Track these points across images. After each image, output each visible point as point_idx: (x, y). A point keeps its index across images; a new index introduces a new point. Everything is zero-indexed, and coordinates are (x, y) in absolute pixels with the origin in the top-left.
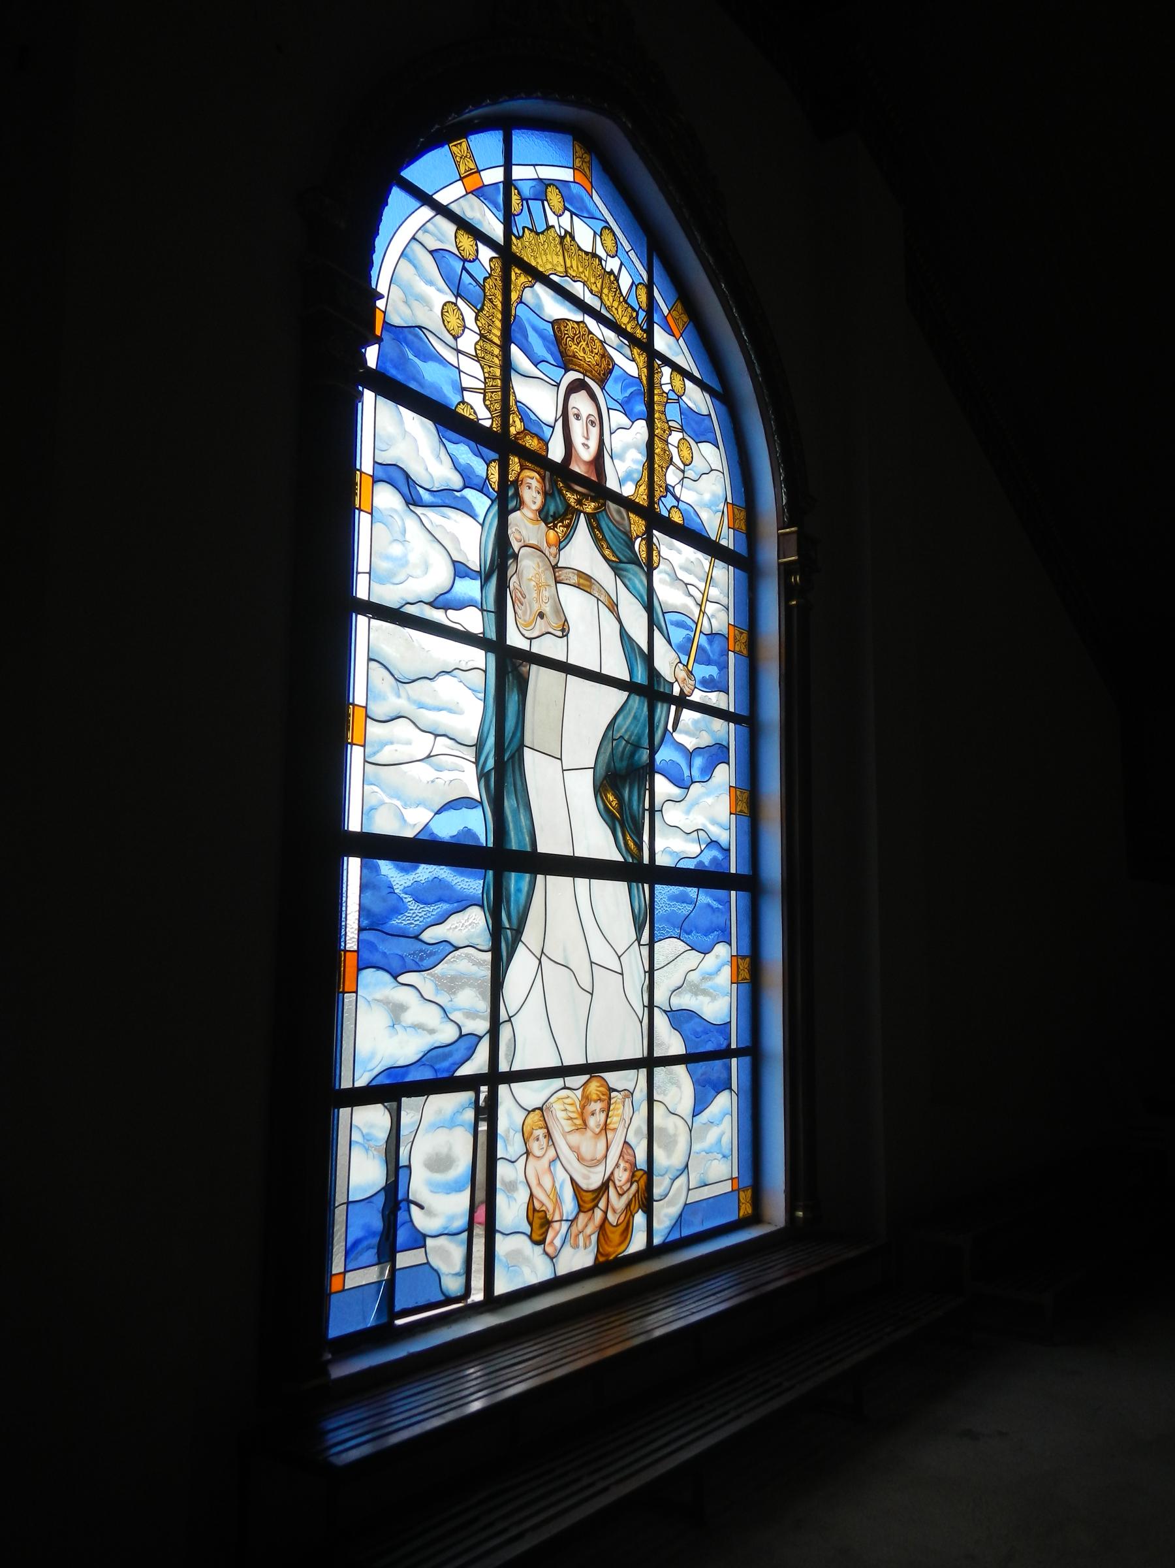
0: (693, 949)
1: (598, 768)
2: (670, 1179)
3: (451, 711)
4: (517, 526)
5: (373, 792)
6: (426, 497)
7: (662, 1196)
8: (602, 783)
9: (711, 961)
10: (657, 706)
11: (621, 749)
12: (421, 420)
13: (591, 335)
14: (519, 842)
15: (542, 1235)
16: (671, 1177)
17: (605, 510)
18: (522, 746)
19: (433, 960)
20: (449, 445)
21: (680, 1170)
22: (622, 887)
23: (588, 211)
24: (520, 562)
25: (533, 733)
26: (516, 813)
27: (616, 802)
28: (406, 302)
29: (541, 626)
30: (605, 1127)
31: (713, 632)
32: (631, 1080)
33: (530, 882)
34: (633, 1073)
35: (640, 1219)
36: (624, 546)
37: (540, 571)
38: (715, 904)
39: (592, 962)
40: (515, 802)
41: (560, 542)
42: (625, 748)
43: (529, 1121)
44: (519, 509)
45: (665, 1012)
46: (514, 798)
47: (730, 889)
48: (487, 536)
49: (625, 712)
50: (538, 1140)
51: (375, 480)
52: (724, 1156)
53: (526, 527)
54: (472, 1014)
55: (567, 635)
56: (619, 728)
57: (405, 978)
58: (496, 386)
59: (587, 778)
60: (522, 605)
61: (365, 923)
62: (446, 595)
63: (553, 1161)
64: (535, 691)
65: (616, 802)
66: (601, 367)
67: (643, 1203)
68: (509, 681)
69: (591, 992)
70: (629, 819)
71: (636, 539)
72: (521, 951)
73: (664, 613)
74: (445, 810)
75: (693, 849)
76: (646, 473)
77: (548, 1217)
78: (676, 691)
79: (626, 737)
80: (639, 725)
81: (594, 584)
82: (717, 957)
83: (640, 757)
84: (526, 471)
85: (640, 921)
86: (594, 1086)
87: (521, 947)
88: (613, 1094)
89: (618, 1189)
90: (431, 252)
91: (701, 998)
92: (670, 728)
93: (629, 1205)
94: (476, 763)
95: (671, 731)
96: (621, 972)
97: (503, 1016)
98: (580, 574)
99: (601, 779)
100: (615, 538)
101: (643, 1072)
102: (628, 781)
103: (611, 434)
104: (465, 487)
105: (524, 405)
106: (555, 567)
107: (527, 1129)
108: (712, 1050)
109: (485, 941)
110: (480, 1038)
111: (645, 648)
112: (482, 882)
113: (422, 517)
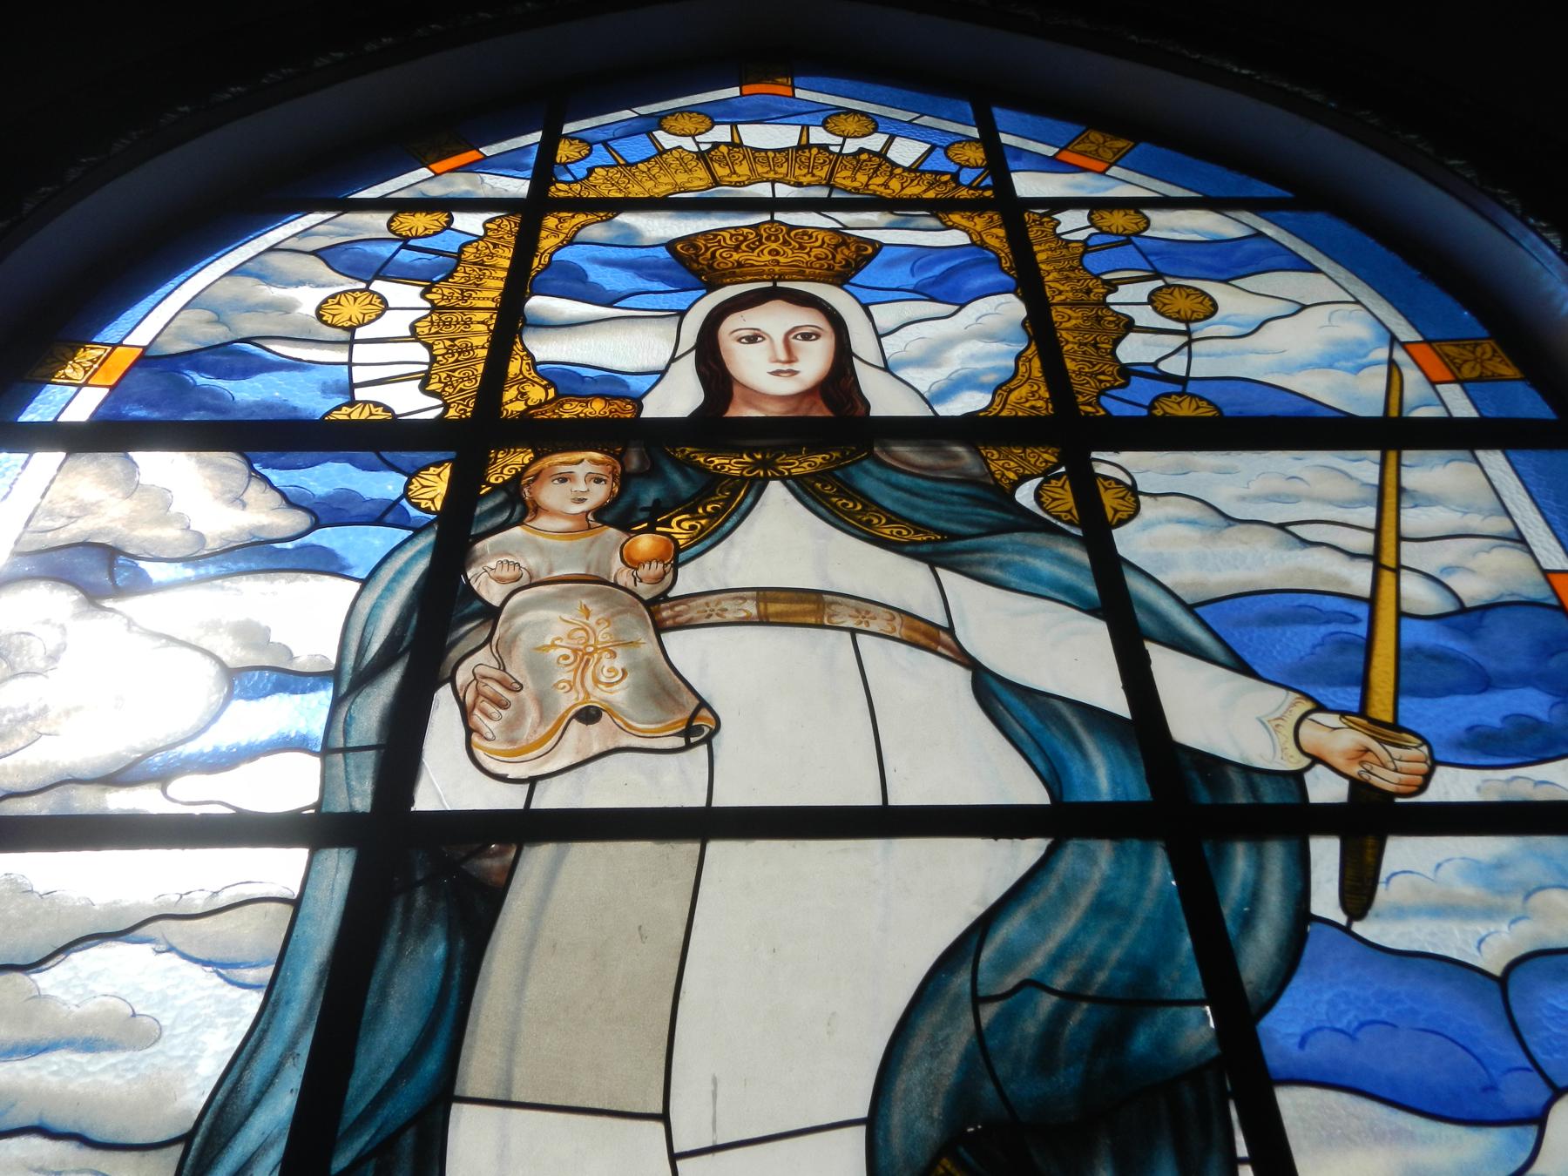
4: (507, 554)
10: (1222, 858)
11: (1031, 1026)
12: (200, 462)
13: (800, 230)
23: (776, 110)
25: (511, 1047)
28: (219, 321)
29: (580, 740)
36: (966, 505)
41: (678, 550)
42: (1058, 1018)
44: (520, 523)
48: (381, 597)
49: (1038, 901)
53: (540, 549)
55: (708, 740)
58: (466, 360)
60: (501, 704)
66: (834, 258)
68: (409, 907)
71: (1016, 485)
73: (1190, 609)
79: (1061, 981)
81: (833, 603)
90: (315, 253)
95: (1342, 919)
98: (764, 594)
99: (922, 1159)
100: (924, 497)
104: (316, 525)
106: (652, 605)
111: (1115, 701)
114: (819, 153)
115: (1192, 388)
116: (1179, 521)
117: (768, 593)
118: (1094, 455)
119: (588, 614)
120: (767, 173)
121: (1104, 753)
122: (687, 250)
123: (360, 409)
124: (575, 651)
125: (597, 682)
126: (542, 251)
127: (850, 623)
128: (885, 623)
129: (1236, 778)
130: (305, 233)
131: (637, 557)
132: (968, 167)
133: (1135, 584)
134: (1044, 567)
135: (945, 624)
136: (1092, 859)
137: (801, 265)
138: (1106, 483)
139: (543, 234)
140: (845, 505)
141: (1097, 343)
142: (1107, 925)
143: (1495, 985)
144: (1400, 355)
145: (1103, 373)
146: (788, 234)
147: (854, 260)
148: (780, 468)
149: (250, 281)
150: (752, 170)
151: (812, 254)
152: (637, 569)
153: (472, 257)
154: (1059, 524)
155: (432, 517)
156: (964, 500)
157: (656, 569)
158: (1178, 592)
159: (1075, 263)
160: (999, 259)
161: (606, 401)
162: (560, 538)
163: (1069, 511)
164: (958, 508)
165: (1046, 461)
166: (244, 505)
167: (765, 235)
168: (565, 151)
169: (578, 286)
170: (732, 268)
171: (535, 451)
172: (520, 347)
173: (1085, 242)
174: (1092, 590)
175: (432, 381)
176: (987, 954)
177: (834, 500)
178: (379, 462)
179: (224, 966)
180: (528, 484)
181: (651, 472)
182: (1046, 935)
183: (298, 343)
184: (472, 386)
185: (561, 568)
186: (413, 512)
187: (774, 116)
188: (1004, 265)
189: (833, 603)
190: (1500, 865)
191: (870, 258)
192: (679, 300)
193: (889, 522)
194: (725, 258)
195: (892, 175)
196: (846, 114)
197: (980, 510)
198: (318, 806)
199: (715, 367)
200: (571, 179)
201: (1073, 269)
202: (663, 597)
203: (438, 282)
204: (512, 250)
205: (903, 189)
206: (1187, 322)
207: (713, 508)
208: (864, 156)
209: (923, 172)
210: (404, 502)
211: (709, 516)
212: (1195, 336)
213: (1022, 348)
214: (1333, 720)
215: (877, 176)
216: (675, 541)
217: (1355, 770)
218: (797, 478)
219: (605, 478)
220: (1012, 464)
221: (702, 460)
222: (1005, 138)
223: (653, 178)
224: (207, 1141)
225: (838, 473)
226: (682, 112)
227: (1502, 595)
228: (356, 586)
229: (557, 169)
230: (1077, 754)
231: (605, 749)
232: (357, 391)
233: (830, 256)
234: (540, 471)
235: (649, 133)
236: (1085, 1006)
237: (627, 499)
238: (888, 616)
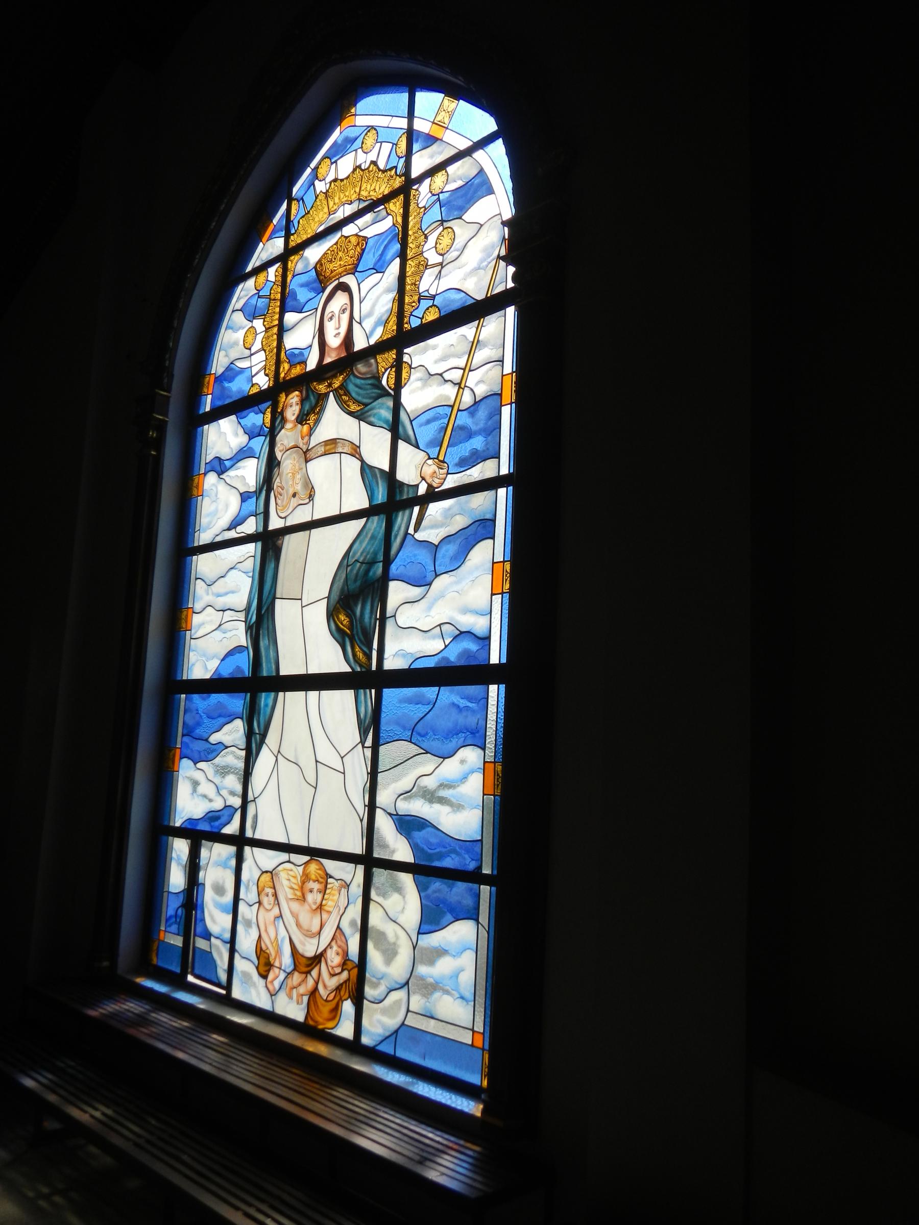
0: (427, 753)
1: (332, 596)
2: (387, 987)
3: (233, 592)
7: (376, 999)
8: (335, 607)
9: (451, 768)
10: (396, 517)
14: (268, 671)
15: (266, 971)
16: (388, 986)
18: (274, 598)
19: (214, 754)
21: (399, 984)
22: (349, 695)
24: (282, 465)
26: (267, 649)
27: (348, 620)
30: (321, 907)
32: (348, 873)
34: (351, 866)
35: (348, 1007)
36: (371, 389)
38: (463, 703)
39: (317, 761)
40: (267, 641)
41: (311, 429)
43: (262, 879)
45: (390, 814)
46: (267, 639)
47: (487, 682)
49: (361, 537)
50: (267, 896)
52: (462, 998)
54: (233, 793)
55: (313, 499)
56: (355, 554)
57: (201, 765)
59: (323, 606)
60: (281, 495)
61: (185, 732)
63: (278, 917)
64: (286, 554)
65: (348, 620)
67: (353, 994)
69: (315, 786)
70: (359, 630)
72: (265, 751)
74: (227, 657)
75: (434, 646)
76: (396, 304)
77: (271, 960)
78: (422, 489)
80: (377, 541)
82: (462, 762)
83: (375, 573)
85: (366, 725)
86: (313, 867)
87: (264, 747)
88: (330, 880)
89: (330, 969)
91: (437, 807)
92: (411, 531)
93: (338, 988)
94: (245, 622)
96: (343, 772)
97: (250, 797)
101: (361, 869)
102: (361, 597)
106: (305, 453)
107: (261, 884)
108: (452, 867)
109: (242, 743)
110: (236, 810)
111: (386, 468)
112: (243, 702)
121: (382, 487)
124: (292, 473)
125: (296, 483)
127: (340, 450)
129: (406, 489)
133: (403, 416)
136: (373, 522)
142: (372, 542)
143: (435, 547)
145: (414, 302)
155: (268, 429)
173: (424, 207)
176: (351, 554)
182: (361, 547)
187: (348, 147)
190: (449, 509)
198: (256, 531)
202: (308, 450)
203: (265, 315)
214: (430, 462)
217: (429, 482)
218: (336, 390)
224: (248, 610)
226: (323, 160)
227: (487, 393)
230: (377, 488)
236: (364, 565)
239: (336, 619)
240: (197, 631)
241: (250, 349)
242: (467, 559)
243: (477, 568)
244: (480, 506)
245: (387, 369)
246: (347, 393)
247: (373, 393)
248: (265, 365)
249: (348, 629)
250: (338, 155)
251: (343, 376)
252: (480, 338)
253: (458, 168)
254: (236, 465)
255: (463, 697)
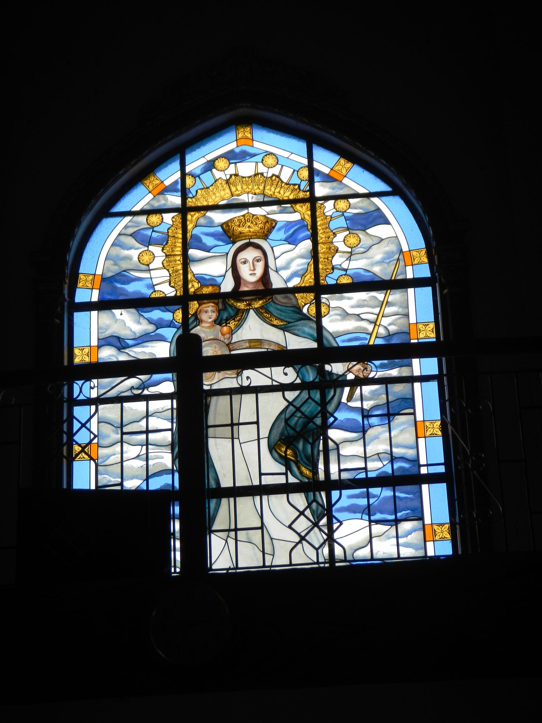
1: (272, 437)
5: (104, 478)
6: (130, 342)
12: (127, 311)
17: (273, 301)
20: (146, 315)
28: (115, 264)
31: (390, 334)
33: (216, 503)
36: (292, 314)
37: (217, 349)
41: (232, 331)
42: (298, 421)
44: (199, 325)
51: (99, 347)
53: (204, 332)
58: (178, 274)
62: (148, 382)
65: (291, 451)
71: (303, 306)
73: (334, 338)
81: (264, 342)
84: (204, 305)
90: (131, 235)
95: (346, 402)
98: (250, 341)
100: (283, 312)
103: (275, 259)
104: (157, 329)
105: (202, 274)
106: (228, 345)
113: (130, 353)
114: (261, 177)
115: (348, 272)
116: (337, 315)
117: (251, 340)
118: (322, 296)
119: (216, 348)
120: (246, 189)
122: (226, 227)
123: (157, 293)
126: (189, 230)
128: (274, 346)
130: (126, 227)
131: (224, 333)
132: (303, 180)
133: (325, 333)
134: (307, 330)
135: (286, 346)
137: (256, 232)
138: (323, 305)
139: (188, 223)
140: (266, 315)
141: (328, 257)
144: (401, 257)
145: (328, 269)
146: (253, 218)
147: (270, 228)
148: (253, 306)
149: (118, 248)
150: (242, 188)
151: (259, 227)
152: (224, 336)
153: (171, 234)
154: (312, 317)
156: (292, 312)
157: (227, 336)
158: (333, 334)
159: (327, 226)
160: (308, 224)
161: (212, 287)
162: (208, 329)
163: (314, 314)
164: (290, 315)
165: (311, 299)
166: (141, 324)
167: (246, 219)
168: (189, 181)
169: (200, 244)
170: (239, 234)
171: (199, 304)
172: (190, 269)
173: (331, 216)
174: (315, 335)
175: (171, 283)
177: (264, 314)
178: (166, 309)
179: (168, 420)
180: (199, 314)
181: (225, 309)
183: (137, 271)
184: (181, 283)
185: (209, 336)
186: (176, 323)
187: (248, 158)
188: (309, 228)
189: (264, 342)
191: (274, 227)
192: (226, 248)
193: (276, 320)
194: (236, 230)
195: (281, 187)
196: (269, 154)
197: (295, 315)
199: (236, 274)
200: (192, 196)
201: (326, 228)
203: (164, 246)
204: (181, 230)
205: (284, 194)
206: (352, 248)
207: (239, 318)
208: (274, 178)
209: (290, 185)
210: (174, 321)
211: (238, 321)
212: (353, 253)
213: (310, 261)
215: (277, 188)
216: (231, 328)
217: (357, 374)
218: (256, 309)
219: (215, 311)
220: (304, 300)
221: (235, 304)
222: (316, 165)
223: (214, 194)
225: (265, 306)
227: (398, 331)
228: (169, 344)
229: (187, 191)
231: (223, 378)
232: (155, 287)
233: (264, 227)
234: (201, 310)
235: (211, 170)
236: (302, 419)
237: (220, 317)
238: (274, 345)
239: (279, 451)
240: (106, 460)
241: (148, 265)
242: (394, 419)
243: (403, 423)
244: (401, 391)
245: (307, 304)
246: (268, 312)
247: (295, 316)
248: (170, 280)
249: (292, 457)
250: (237, 160)
251: (262, 301)
252: (389, 300)
253: (358, 202)
254: (141, 344)
255: (402, 492)
